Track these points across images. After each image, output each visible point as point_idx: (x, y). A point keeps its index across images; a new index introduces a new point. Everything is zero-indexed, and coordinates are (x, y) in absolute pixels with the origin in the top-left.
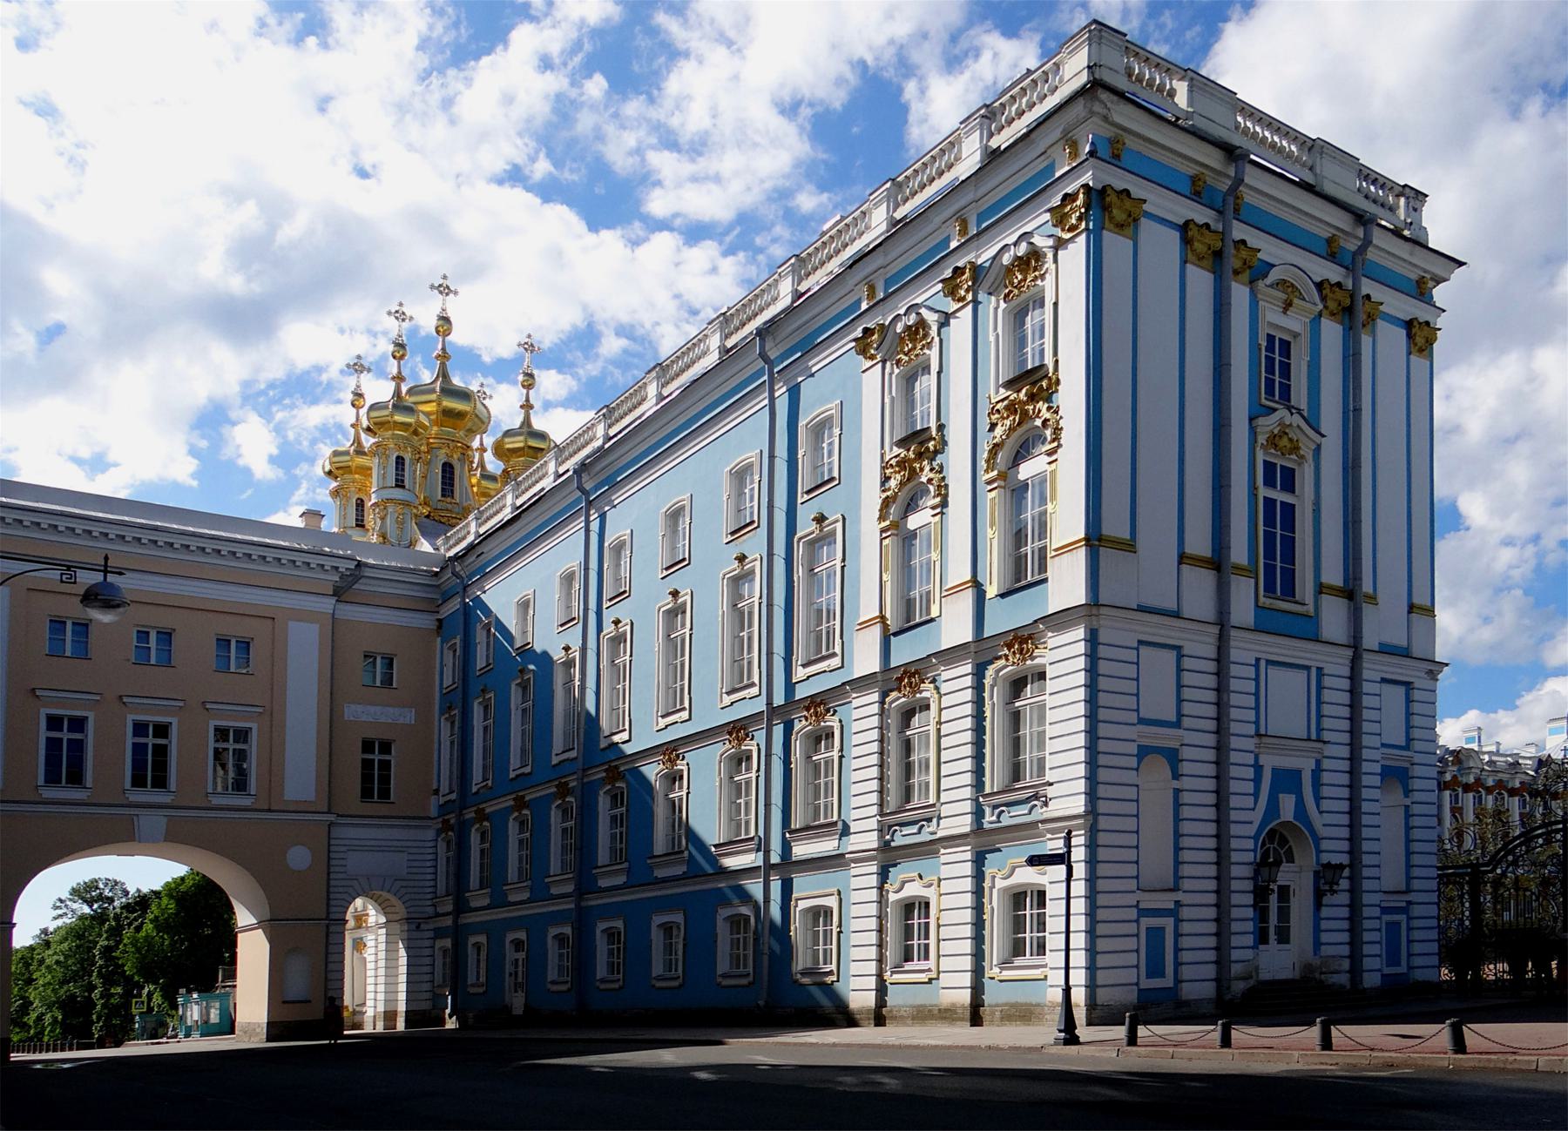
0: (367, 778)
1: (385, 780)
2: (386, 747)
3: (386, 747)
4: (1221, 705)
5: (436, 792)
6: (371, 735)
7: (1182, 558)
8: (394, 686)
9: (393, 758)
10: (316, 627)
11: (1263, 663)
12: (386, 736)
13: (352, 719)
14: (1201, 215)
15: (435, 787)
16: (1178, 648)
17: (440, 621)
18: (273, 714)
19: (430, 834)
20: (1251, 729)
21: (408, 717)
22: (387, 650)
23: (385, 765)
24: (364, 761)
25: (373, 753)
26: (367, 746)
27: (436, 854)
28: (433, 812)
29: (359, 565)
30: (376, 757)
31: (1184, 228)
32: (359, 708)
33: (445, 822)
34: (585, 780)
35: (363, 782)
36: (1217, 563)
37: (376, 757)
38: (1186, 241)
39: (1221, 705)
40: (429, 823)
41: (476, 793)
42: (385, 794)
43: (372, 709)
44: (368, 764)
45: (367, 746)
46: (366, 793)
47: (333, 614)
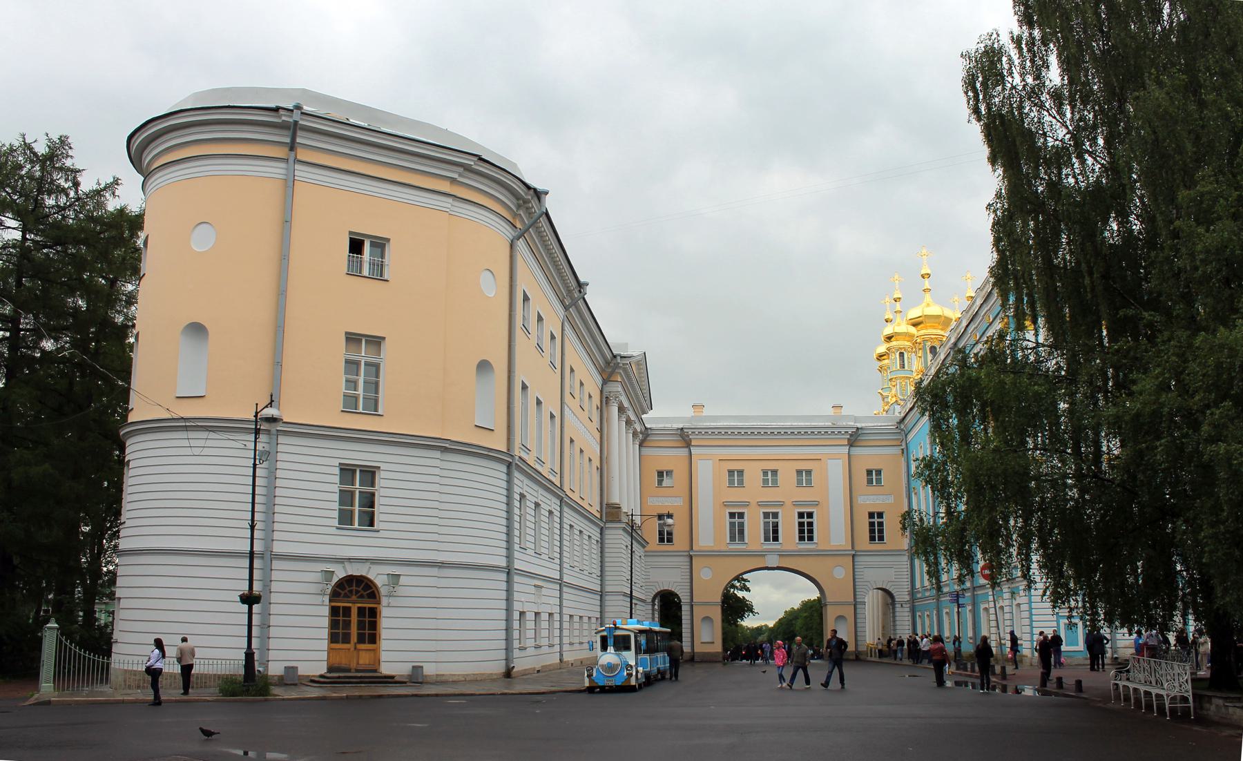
0: (872, 531)
1: (881, 531)
2: (880, 515)
3: (880, 515)
8: (883, 484)
9: (884, 520)
17: (903, 449)
21: (891, 500)
23: (881, 524)
24: (870, 522)
25: (874, 518)
26: (871, 515)
29: (858, 428)
30: (876, 520)
35: (870, 533)
42: (881, 538)
46: (872, 539)
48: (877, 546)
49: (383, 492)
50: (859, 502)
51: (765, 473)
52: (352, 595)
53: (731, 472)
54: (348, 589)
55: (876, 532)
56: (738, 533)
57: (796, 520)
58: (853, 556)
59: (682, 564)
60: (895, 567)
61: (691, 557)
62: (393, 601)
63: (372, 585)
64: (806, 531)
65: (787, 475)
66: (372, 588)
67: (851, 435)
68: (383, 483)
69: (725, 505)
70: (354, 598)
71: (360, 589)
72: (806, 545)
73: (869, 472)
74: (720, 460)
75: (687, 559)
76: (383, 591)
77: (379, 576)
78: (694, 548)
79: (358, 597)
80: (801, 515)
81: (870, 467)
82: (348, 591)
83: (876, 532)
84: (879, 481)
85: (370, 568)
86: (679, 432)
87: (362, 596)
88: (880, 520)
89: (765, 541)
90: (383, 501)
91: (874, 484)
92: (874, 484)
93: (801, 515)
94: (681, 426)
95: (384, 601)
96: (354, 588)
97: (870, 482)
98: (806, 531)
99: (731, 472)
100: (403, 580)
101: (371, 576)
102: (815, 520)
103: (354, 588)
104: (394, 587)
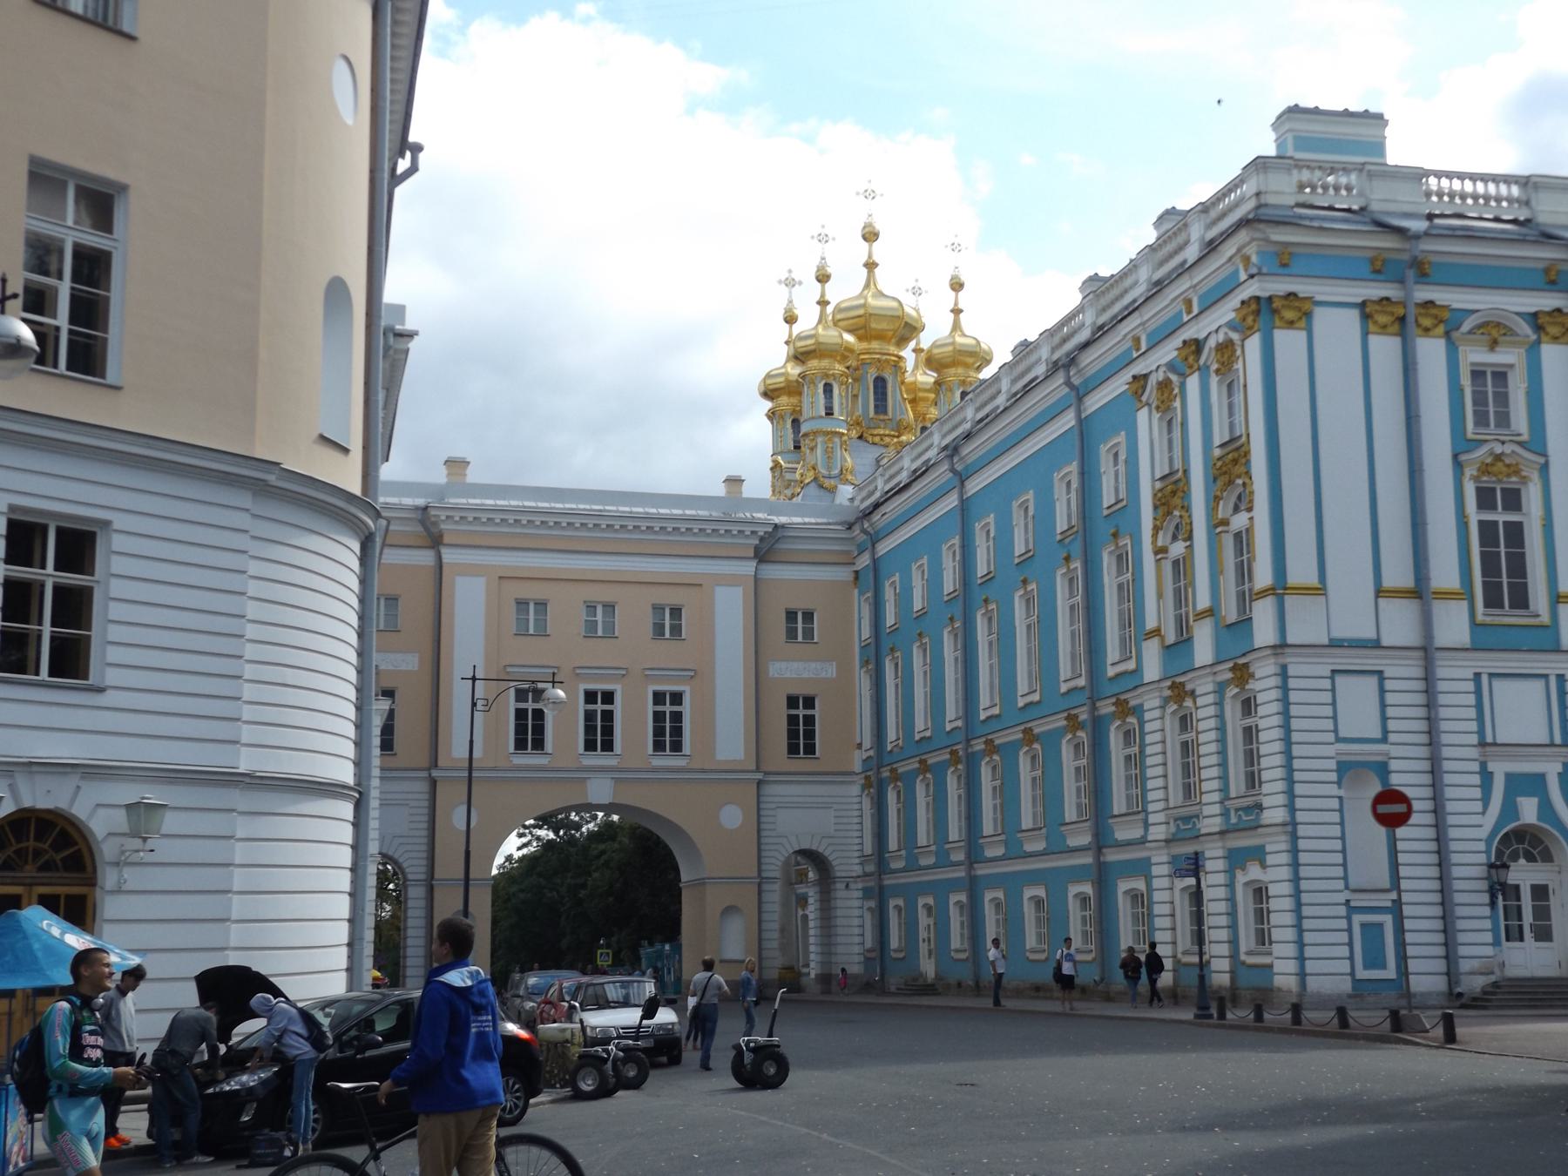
0: (793, 734)
1: (810, 735)
2: (809, 702)
3: (809, 702)
4: (1432, 721)
5: (860, 746)
6: (794, 691)
7: (1380, 592)
9: (817, 712)
10: (739, 591)
11: (1485, 679)
12: (808, 691)
13: (776, 676)
14: (1375, 291)
15: (858, 741)
16: (1381, 672)
18: (701, 674)
19: (855, 790)
20: (1474, 739)
21: (830, 671)
22: (809, 606)
23: (810, 720)
26: (792, 702)
27: (861, 809)
28: (858, 767)
29: (776, 526)
30: (801, 712)
31: (1363, 305)
32: (784, 665)
33: (867, 778)
34: (970, 750)
36: (1419, 592)
37: (801, 712)
38: (1366, 317)
39: (1432, 721)
40: (855, 778)
41: (891, 751)
42: (810, 749)
43: (795, 665)
44: (792, 720)
45: (792, 702)
46: (793, 749)
47: (755, 576)
48: (801, 764)
49: (117, 588)
50: (771, 674)
51: (591, 608)
52: (26, 862)
53: (522, 604)
54: (15, 847)
55: (801, 738)
56: (530, 731)
57: (650, 708)
58: (759, 783)
59: (410, 796)
60: (835, 806)
61: (433, 783)
62: (133, 878)
63: (76, 835)
64: (668, 734)
65: (634, 618)
66: (76, 844)
67: (762, 539)
68: (119, 565)
69: (578, 674)
70: (30, 871)
71: (46, 846)
72: (668, 761)
73: (791, 616)
74: (500, 578)
75: (423, 787)
76: (107, 850)
77: (102, 812)
78: (440, 763)
79: (41, 869)
80: (659, 698)
81: (793, 606)
82: (15, 852)
83: (801, 738)
84: (809, 634)
85: (78, 787)
86: (418, 515)
87: (47, 867)
88: (809, 712)
89: (586, 750)
90: (116, 610)
91: (800, 638)
92: (800, 638)
93: (659, 698)
94: (421, 502)
95: (108, 878)
96: (32, 843)
97: (791, 634)
98: (668, 734)
99: (522, 604)
100: (171, 822)
101: (80, 811)
102: (686, 709)
103: (32, 843)
104: (145, 839)
